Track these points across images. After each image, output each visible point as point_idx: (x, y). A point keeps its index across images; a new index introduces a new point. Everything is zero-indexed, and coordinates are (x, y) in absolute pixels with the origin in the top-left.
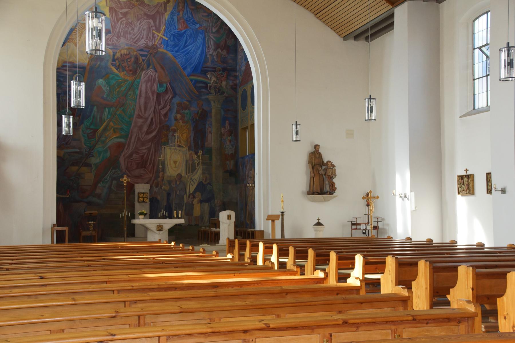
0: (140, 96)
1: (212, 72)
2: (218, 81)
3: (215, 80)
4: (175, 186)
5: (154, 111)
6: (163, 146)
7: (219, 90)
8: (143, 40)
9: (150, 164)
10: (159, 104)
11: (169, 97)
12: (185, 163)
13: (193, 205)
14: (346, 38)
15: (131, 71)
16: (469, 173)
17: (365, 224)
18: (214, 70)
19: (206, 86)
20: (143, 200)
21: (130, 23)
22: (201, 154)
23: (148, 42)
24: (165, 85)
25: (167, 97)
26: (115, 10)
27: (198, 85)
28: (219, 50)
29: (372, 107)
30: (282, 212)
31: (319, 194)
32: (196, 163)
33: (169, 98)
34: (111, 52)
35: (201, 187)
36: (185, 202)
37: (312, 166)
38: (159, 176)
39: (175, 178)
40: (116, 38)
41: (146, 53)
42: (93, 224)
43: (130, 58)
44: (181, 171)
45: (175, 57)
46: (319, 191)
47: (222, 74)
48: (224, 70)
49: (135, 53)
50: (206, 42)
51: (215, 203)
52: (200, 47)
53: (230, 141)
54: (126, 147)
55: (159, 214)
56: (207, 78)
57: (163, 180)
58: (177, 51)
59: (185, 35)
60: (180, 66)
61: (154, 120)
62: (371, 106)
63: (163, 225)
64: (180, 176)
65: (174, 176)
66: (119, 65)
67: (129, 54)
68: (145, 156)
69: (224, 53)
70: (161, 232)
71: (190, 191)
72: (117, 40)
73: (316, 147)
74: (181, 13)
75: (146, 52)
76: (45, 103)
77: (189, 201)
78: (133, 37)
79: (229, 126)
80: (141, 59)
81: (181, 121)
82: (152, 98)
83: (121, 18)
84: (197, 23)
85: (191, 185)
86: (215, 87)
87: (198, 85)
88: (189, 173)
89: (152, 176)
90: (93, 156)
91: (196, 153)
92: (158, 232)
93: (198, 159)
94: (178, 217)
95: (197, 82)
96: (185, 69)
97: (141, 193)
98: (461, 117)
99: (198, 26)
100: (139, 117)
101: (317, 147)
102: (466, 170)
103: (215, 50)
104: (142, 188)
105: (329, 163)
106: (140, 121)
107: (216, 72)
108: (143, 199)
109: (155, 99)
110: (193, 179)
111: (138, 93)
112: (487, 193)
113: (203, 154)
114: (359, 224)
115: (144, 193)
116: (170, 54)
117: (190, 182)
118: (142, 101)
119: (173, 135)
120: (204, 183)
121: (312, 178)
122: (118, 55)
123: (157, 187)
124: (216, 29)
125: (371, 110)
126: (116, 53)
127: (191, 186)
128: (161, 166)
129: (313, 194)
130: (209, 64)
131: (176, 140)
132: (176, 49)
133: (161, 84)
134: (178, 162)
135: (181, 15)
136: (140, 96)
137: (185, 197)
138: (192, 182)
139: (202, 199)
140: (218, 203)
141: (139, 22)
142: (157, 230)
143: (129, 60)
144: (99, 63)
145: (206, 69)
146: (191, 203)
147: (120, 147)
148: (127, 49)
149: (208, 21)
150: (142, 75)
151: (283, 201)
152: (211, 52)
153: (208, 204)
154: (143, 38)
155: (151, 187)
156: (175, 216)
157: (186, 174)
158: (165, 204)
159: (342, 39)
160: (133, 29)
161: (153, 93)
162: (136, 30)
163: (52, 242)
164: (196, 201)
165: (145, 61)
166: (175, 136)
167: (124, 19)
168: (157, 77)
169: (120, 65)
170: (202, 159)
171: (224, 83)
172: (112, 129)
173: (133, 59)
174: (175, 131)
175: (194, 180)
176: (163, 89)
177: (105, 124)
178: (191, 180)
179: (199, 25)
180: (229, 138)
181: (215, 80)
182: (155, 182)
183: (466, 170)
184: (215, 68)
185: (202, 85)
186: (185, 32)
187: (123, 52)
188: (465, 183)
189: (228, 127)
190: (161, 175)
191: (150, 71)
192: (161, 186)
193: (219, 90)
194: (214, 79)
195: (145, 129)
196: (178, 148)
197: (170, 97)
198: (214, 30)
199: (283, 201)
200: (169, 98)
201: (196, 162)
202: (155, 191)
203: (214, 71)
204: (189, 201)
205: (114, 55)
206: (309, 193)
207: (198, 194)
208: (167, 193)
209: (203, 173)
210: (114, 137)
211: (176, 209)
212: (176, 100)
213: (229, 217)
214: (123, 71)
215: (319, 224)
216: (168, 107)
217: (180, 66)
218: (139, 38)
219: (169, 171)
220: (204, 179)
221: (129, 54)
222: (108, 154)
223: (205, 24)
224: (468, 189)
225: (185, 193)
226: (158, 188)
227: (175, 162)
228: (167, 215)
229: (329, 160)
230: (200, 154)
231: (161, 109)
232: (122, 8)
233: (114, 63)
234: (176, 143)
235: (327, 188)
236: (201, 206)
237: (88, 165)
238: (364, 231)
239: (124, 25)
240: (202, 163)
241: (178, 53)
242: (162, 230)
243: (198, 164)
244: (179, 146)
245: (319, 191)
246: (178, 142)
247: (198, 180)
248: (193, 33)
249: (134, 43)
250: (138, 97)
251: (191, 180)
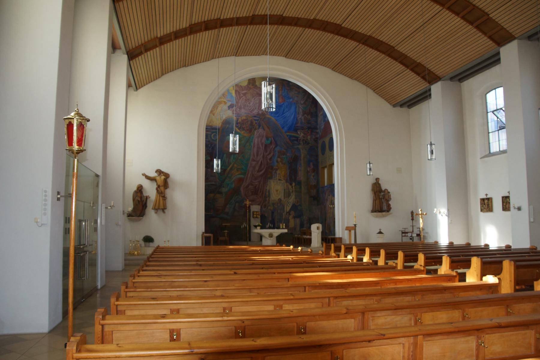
0: (254, 146)
1: (302, 130)
2: (305, 136)
3: (303, 135)
5: (263, 156)
6: (269, 180)
7: (306, 141)
8: (256, 110)
9: (260, 192)
10: (266, 152)
11: (273, 147)
12: (283, 191)
13: (289, 220)
14: (394, 106)
15: (248, 130)
16: (488, 197)
17: (411, 232)
18: (302, 128)
19: (297, 139)
20: (256, 217)
21: (247, 99)
22: (294, 185)
23: (259, 111)
24: (270, 139)
25: (271, 147)
26: (239, 92)
27: (292, 139)
28: (306, 115)
29: (433, 150)
30: (355, 225)
31: (379, 212)
32: (291, 192)
33: (273, 148)
34: (235, 118)
35: (294, 207)
36: (284, 218)
37: (374, 192)
40: (239, 109)
41: (258, 118)
42: (227, 232)
43: (247, 122)
44: (281, 196)
45: (277, 120)
46: (379, 210)
47: (307, 131)
48: (309, 128)
49: (251, 119)
50: (297, 110)
52: (292, 114)
53: (313, 176)
54: (245, 181)
56: (298, 134)
57: (269, 203)
58: (277, 117)
59: (283, 106)
60: (280, 126)
61: (263, 162)
62: (432, 149)
63: (273, 233)
64: (280, 200)
66: (240, 127)
67: (246, 120)
68: (257, 187)
69: (309, 117)
70: (272, 238)
72: (239, 111)
73: (377, 179)
74: (281, 92)
75: (258, 117)
76: (198, 152)
78: (250, 108)
79: (312, 166)
80: (254, 122)
81: (280, 163)
82: (261, 148)
83: (242, 97)
84: (291, 98)
86: (303, 140)
87: (292, 139)
88: (286, 198)
90: (223, 187)
91: (291, 184)
92: (269, 238)
93: (292, 189)
94: (283, 228)
95: (291, 136)
96: (283, 128)
97: (255, 212)
98: (481, 158)
99: (291, 100)
100: (253, 160)
101: (378, 179)
102: (487, 195)
103: (303, 115)
104: (255, 208)
105: (386, 191)
106: (254, 163)
107: (304, 130)
109: (264, 148)
111: (252, 144)
112: (503, 210)
113: (295, 185)
114: (407, 233)
115: (257, 212)
116: (273, 119)
117: (287, 205)
118: (255, 150)
119: (276, 173)
120: (296, 204)
121: (374, 201)
122: (240, 120)
123: (265, 207)
124: (303, 102)
125: (432, 152)
126: (239, 119)
127: (287, 206)
128: (267, 194)
129: (375, 212)
130: (299, 125)
131: (278, 176)
132: (277, 115)
133: (267, 138)
134: (279, 191)
135: (280, 93)
136: (254, 146)
138: (288, 204)
141: (253, 99)
142: (269, 237)
143: (247, 123)
144: (227, 126)
145: (297, 128)
147: (241, 180)
148: (245, 116)
149: (298, 97)
150: (255, 133)
151: (355, 217)
152: (300, 117)
154: (256, 109)
155: (261, 207)
156: (281, 227)
157: (284, 199)
158: (270, 219)
159: (392, 106)
160: (250, 103)
161: (262, 144)
162: (251, 103)
163: (202, 245)
164: (291, 217)
165: (257, 124)
166: (277, 173)
167: (244, 97)
168: (265, 133)
169: (241, 127)
170: (295, 189)
171: (309, 137)
172: (236, 169)
173: (249, 123)
174: (277, 170)
175: (290, 203)
176: (269, 142)
177: (231, 166)
179: (293, 99)
180: (313, 174)
181: (303, 135)
183: (487, 195)
184: (303, 127)
185: (294, 138)
186: (283, 104)
187: (243, 118)
188: (486, 204)
189: (312, 166)
191: (261, 130)
193: (306, 141)
194: (302, 134)
195: (257, 168)
196: (279, 181)
197: (274, 147)
198: (302, 102)
199: (355, 217)
200: (273, 148)
201: (291, 191)
203: (303, 130)
205: (237, 121)
206: (373, 211)
207: (293, 213)
209: (296, 198)
210: (237, 174)
212: (278, 149)
213: (318, 228)
214: (243, 130)
215: (380, 233)
216: (272, 154)
217: (280, 126)
218: (253, 109)
221: (247, 119)
222: (233, 186)
223: (296, 99)
224: (488, 207)
225: (284, 211)
227: (277, 191)
229: (387, 189)
230: (294, 185)
231: (268, 155)
232: (243, 90)
233: (237, 125)
234: (277, 178)
235: (385, 208)
237: (221, 193)
238: (411, 238)
239: (244, 101)
240: (295, 191)
241: (279, 118)
242: (272, 237)
243: (292, 192)
244: (279, 180)
245: (379, 210)
246: (278, 177)
247: (292, 203)
248: (289, 104)
249: (250, 112)
250: (253, 147)
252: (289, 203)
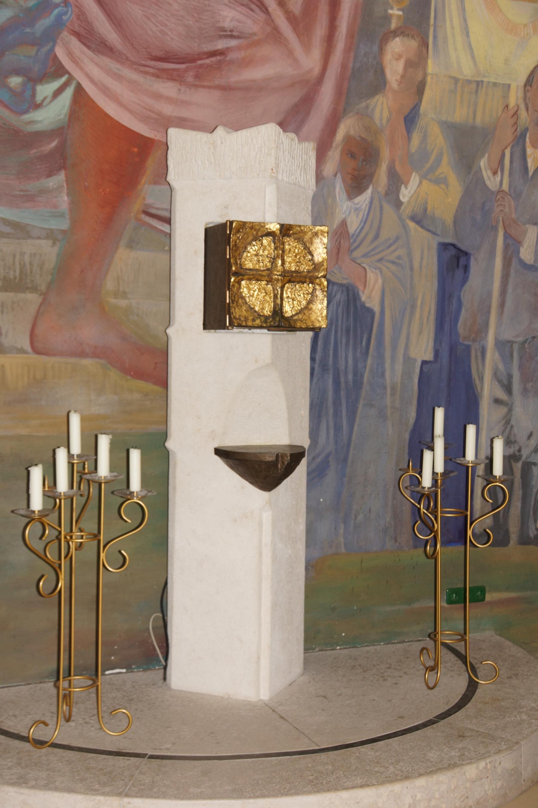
4: (505, 187)
38: (380, 71)
39: (512, 103)
89: (317, 70)
190: (400, 66)
202: (344, 224)
208: (444, 247)
211: (508, 389)
219: (466, 32)
226: (364, 199)
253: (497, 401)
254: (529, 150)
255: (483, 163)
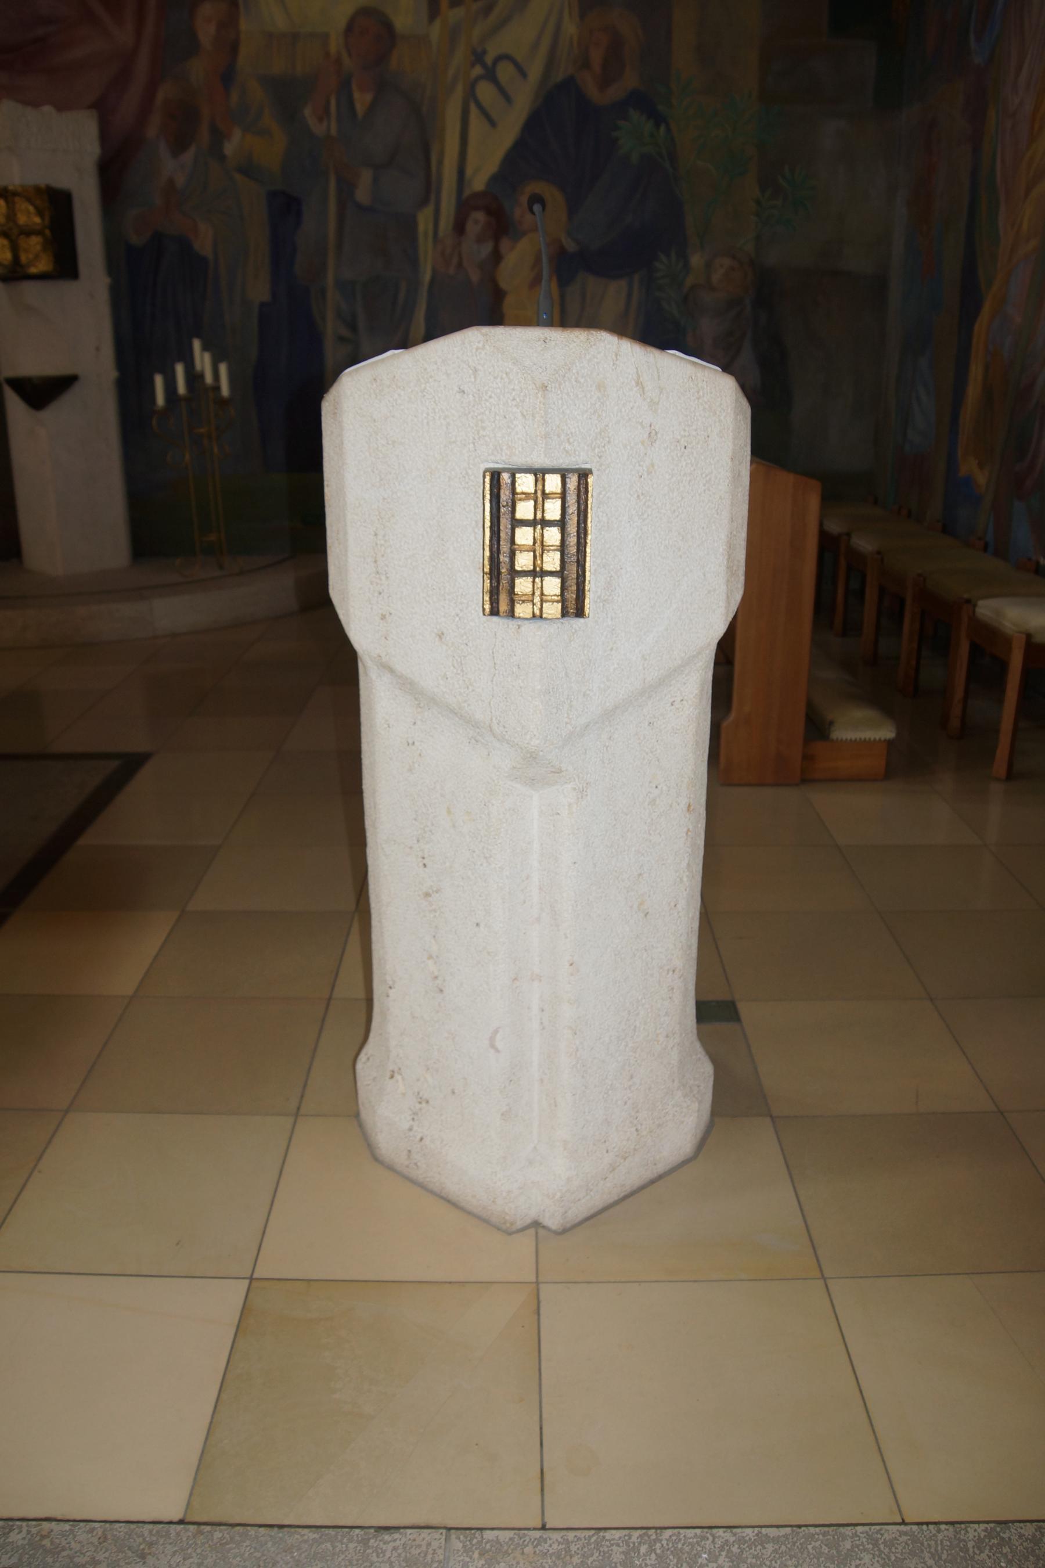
4: (334, 131)
51: (689, 281)
55: (159, 381)
57: (227, 76)
65: (325, 37)
71: (469, 171)
77: (460, 265)
85: (474, 110)
108: (15, 249)
110: (489, 59)
123: (179, 144)
137: (421, 228)
138: (486, 91)
139: (571, 246)
140: (716, 278)
146: (475, 276)
153: (623, 283)
158: (259, 291)
175: (505, 72)
178: (478, 70)
182: (160, 96)
192: (218, 137)
204: (460, 265)
211: (353, 327)
220: (597, 56)
225: (429, 191)
226: (188, 156)
228: (225, 391)
236: (562, 297)
247: (535, 71)
251: (478, 70)
252: (491, 75)
253: (342, 339)
254: (357, 95)
255: (307, 112)
